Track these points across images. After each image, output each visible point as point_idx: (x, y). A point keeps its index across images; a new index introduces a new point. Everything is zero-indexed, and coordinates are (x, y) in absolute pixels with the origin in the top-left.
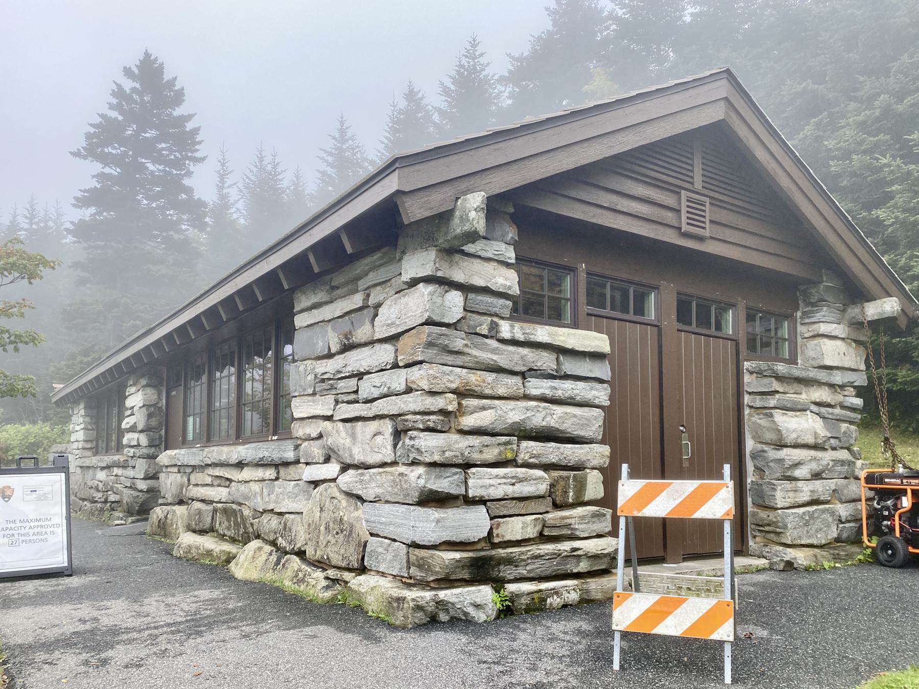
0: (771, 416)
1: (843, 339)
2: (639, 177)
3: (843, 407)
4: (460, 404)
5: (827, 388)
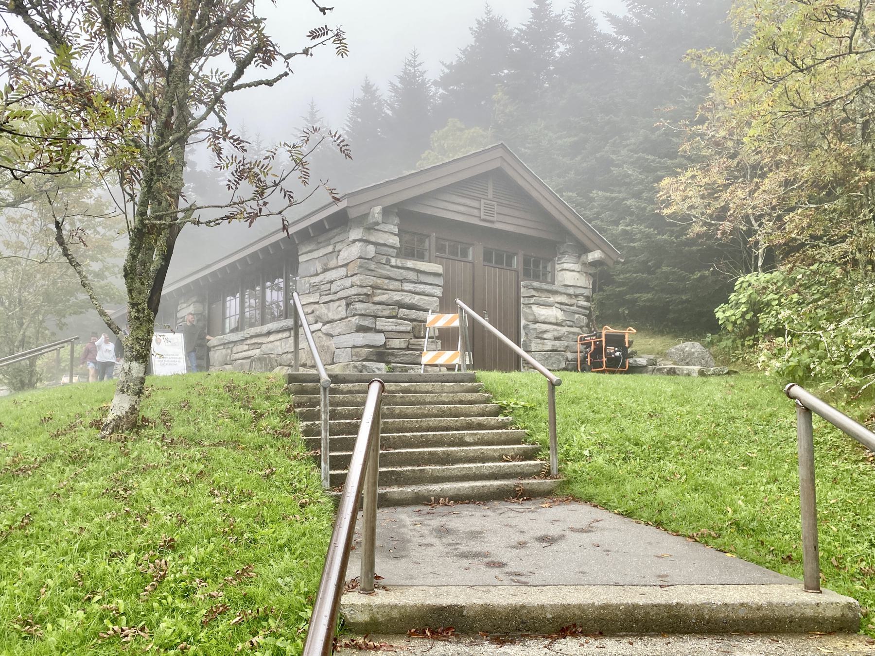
0: (531, 307)
1: (578, 272)
3: (577, 306)
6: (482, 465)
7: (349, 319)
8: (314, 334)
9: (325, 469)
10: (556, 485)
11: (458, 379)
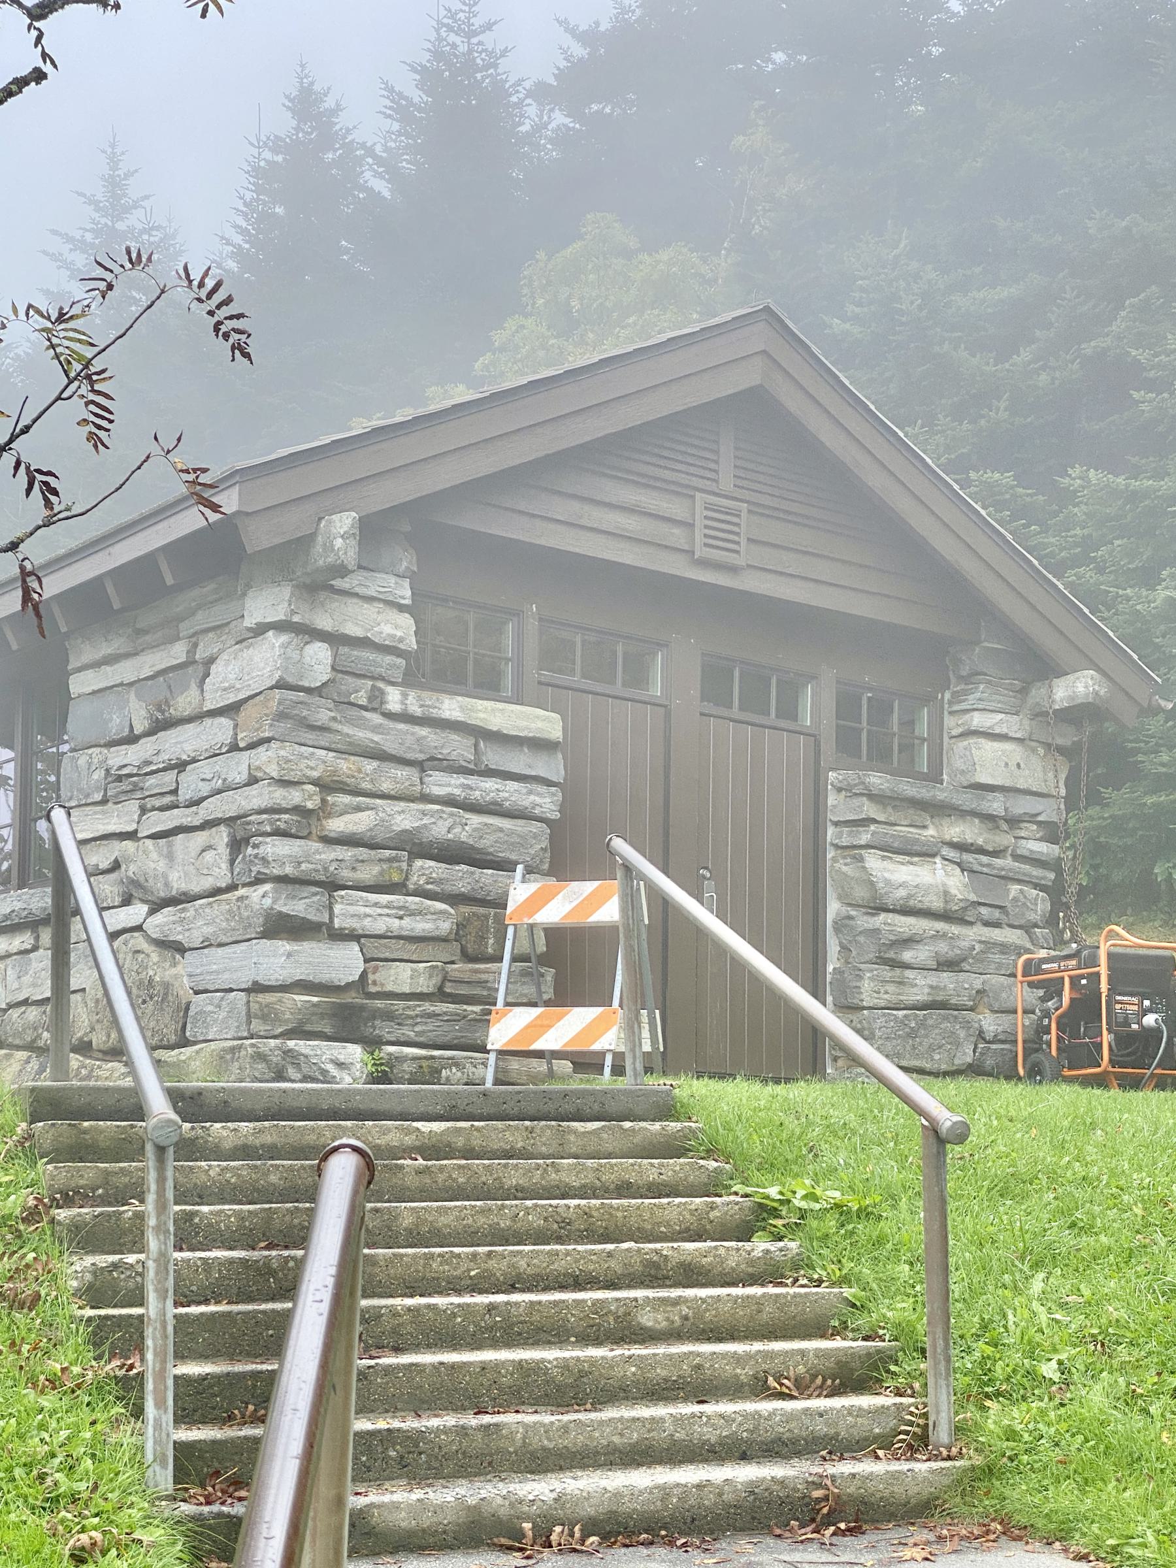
0: (861, 859)
2: (619, 475)
3: (1017, 857)
4: (324, 801)
5: (977, 821)
6: (697, 1408)
7: (242, 892)
8: (116, 944)
9: (158, 1425)
10: (946, 1481)
11: (612, 1107)
